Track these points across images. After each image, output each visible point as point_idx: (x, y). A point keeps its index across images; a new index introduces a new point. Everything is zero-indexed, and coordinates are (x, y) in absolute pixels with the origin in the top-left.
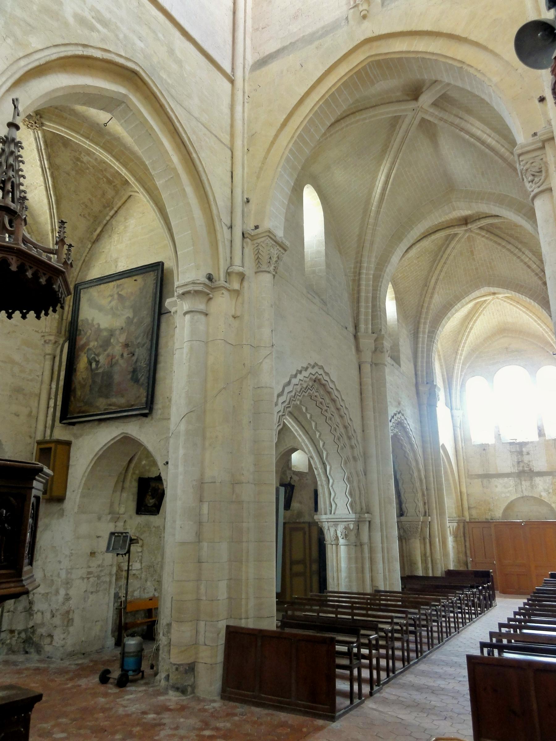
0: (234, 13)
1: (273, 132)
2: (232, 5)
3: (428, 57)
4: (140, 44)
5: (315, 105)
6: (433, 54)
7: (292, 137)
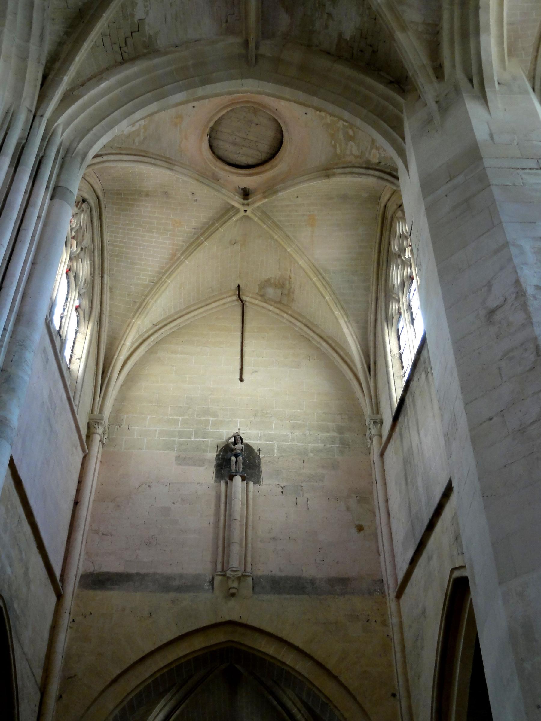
0: (76, 503)
1: (100, 688)
2: (74, 493)
3: (294, 673)
4: (9, 570)
5: (158, 671)
6: (300, 674)
7: (122, 701)
